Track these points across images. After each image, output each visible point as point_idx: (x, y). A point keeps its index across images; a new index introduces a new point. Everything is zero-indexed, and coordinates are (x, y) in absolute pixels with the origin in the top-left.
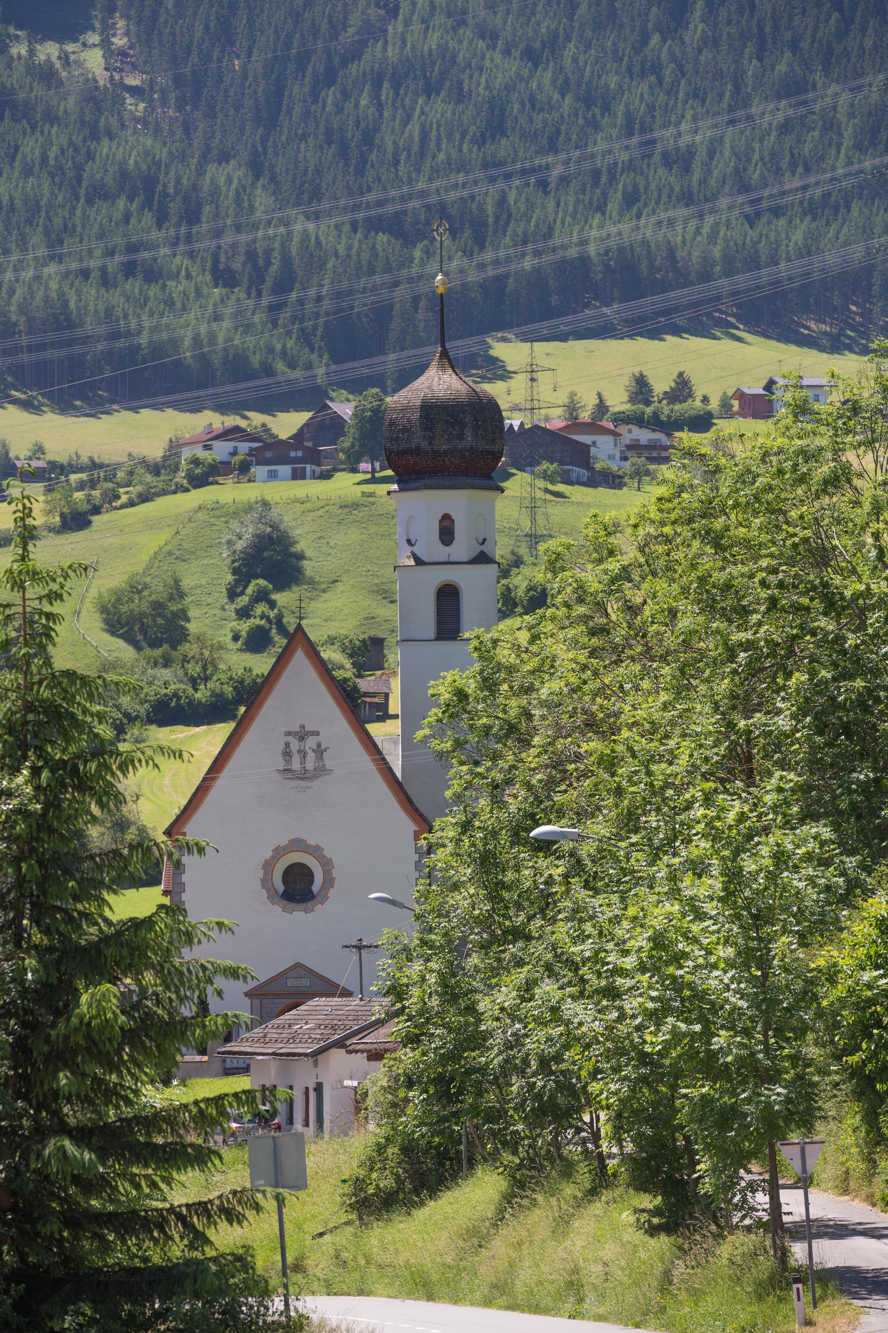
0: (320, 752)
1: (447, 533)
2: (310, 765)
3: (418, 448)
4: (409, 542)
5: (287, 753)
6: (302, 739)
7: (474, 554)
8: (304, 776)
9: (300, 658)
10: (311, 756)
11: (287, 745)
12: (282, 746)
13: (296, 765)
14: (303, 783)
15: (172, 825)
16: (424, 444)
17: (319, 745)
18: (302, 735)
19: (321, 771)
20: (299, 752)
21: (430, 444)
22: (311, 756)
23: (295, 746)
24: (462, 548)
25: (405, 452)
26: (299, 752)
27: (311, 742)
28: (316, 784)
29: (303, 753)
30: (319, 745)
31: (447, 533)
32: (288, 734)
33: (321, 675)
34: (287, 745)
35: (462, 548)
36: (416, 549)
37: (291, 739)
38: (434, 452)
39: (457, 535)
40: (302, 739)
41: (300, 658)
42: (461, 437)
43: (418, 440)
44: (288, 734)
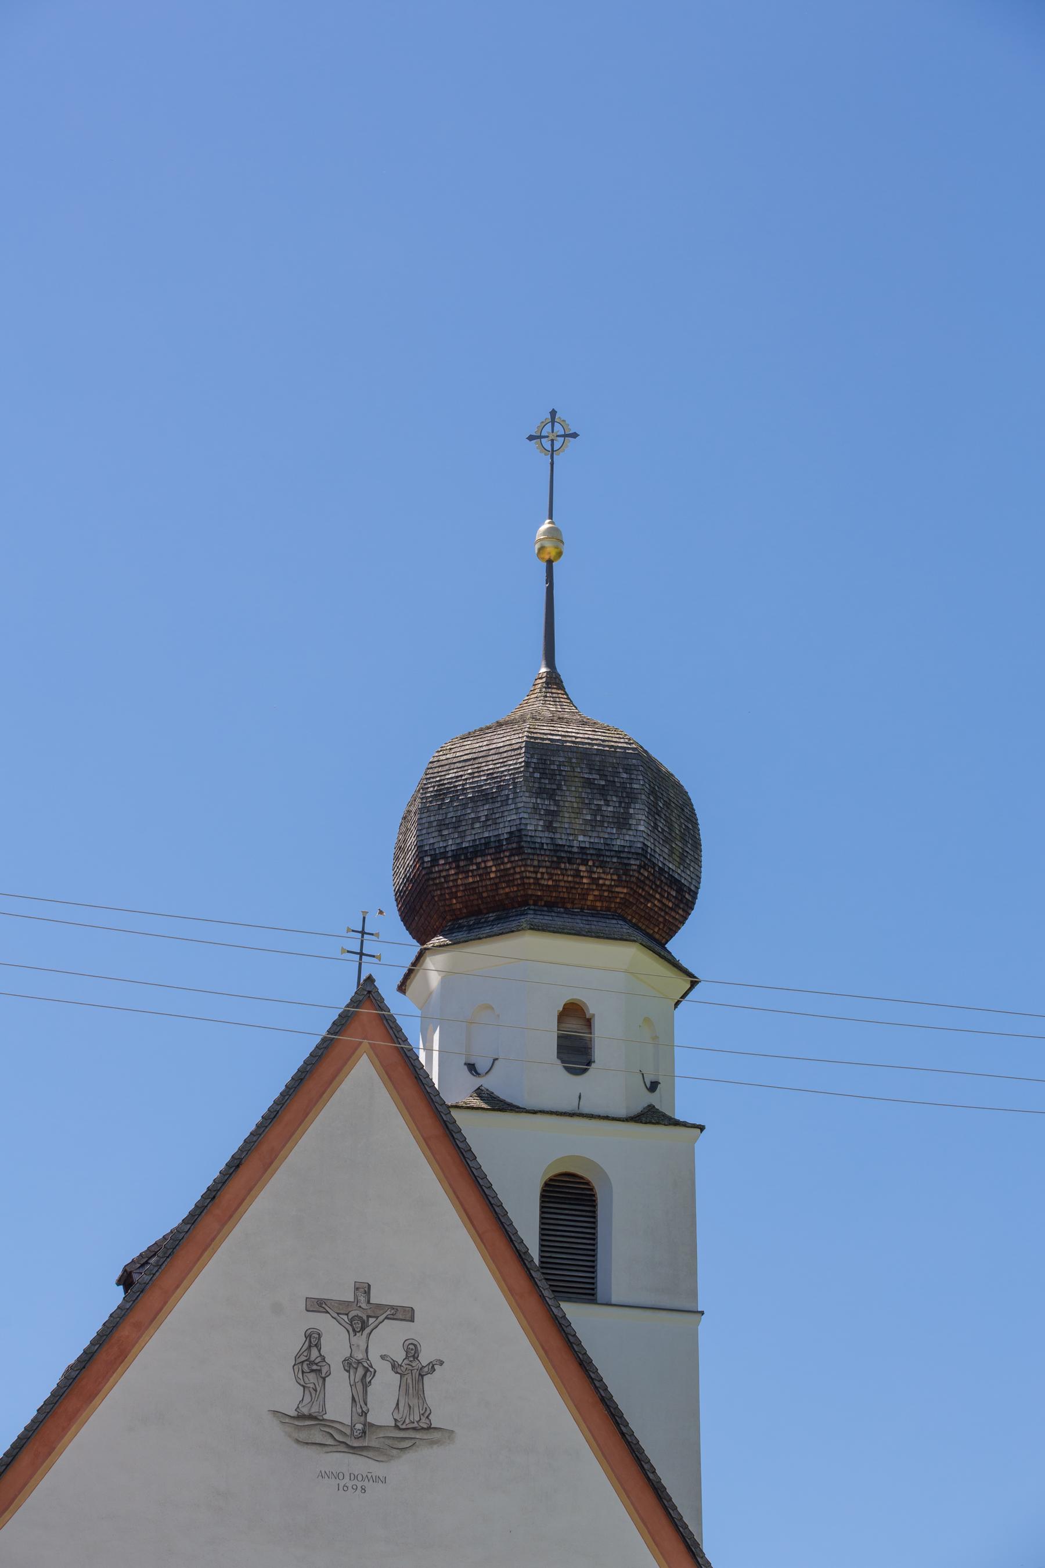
0: (414, 1370)
1: (575, 1051)
2: (382, 1411)
3: (518, 835)
4: (472, 1068)
5: (310, 1365)
6: (359, 1325)
7: (637, 1108)
8: (359, 1438)
9: (363, 1078)
10: (385, 1388)
11: (313, 1340)
12: (297, 1342)
13: (338, 1405)
14: (358, 1464)
15: (143, 1261)
16: (534, 826)
17: (412, 1351)
18: (362, 1315)
19: (416, 1430)
20: (349, 1365)
21: (549, 827)
22: (385, 1388)
23: (336, 1343)
24: (608, 1085)
25: (479, 850)
26: (349, 1365)
27: (387, 1341)
28: (401, 1469)
29: (361, 1371)
30: (412, 1351)
31: (575, 1051)
32: (318, 1305)
33: (426, 1141)
34: (313, 1340)
35: (608, 1085)
36: (489, 1083)
37: (323, 1322)
38: (557, 848)
39: (600, 1052)
40: (359, 1325)
41: (363, 1078)
42: (623, 822)
43: (522, 814)
44: (318, 1305)
